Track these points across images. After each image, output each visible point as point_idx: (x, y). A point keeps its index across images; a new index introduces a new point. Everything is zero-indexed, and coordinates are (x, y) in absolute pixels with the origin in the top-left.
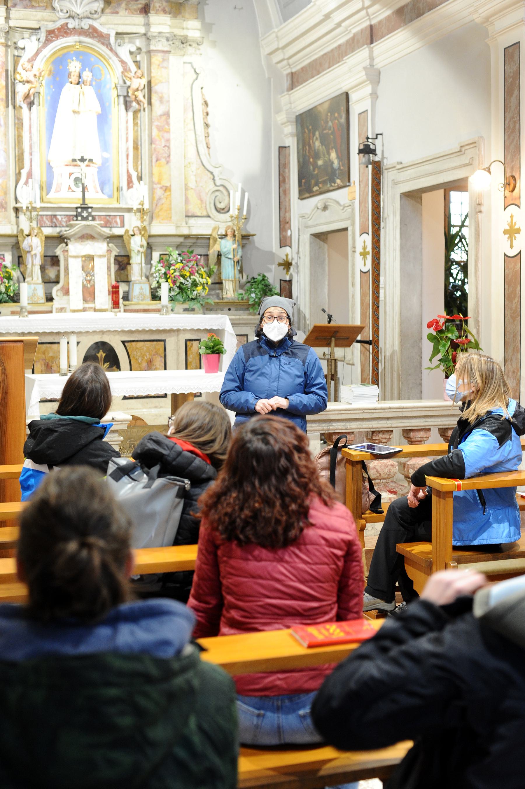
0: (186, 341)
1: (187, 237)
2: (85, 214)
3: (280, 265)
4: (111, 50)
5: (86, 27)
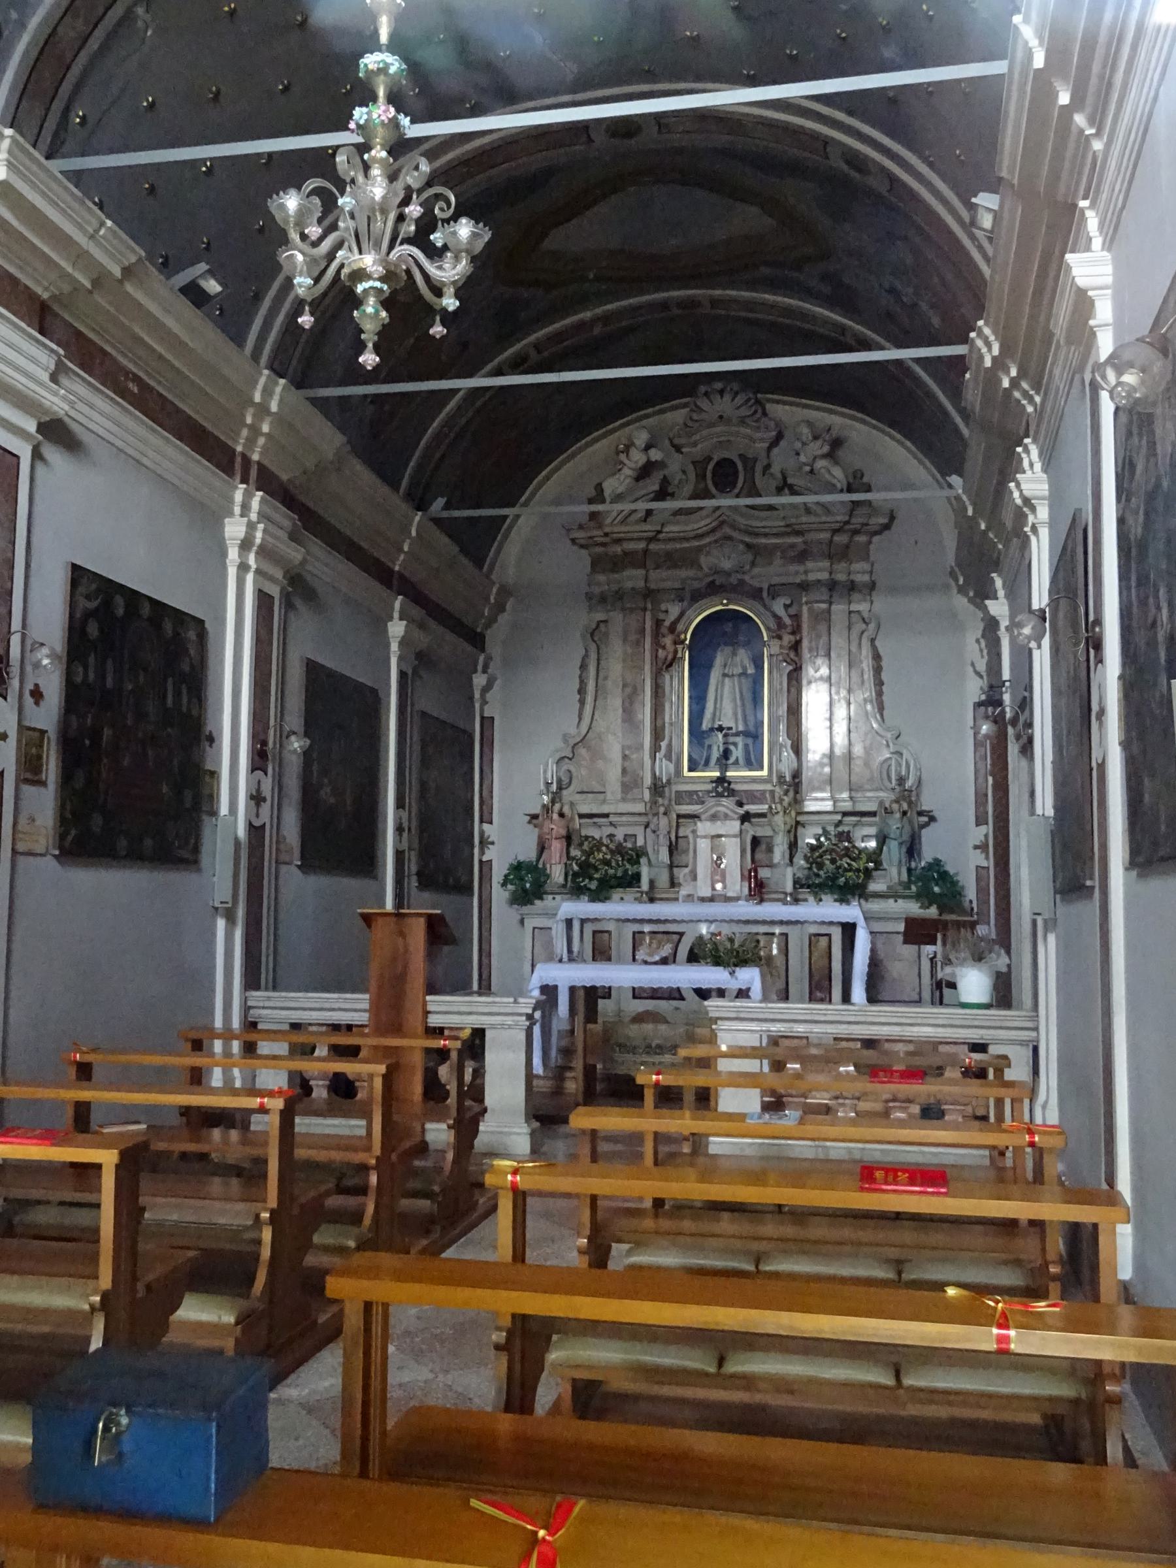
0: (634, 933)
1: (845, 814)
2: (720, 789)
3: (976, 847)
4: (765, 606)
5: (735, 582)
